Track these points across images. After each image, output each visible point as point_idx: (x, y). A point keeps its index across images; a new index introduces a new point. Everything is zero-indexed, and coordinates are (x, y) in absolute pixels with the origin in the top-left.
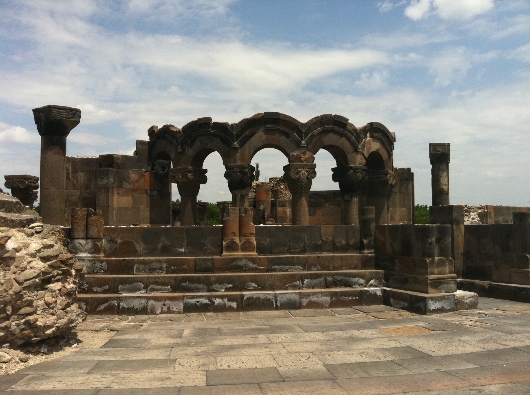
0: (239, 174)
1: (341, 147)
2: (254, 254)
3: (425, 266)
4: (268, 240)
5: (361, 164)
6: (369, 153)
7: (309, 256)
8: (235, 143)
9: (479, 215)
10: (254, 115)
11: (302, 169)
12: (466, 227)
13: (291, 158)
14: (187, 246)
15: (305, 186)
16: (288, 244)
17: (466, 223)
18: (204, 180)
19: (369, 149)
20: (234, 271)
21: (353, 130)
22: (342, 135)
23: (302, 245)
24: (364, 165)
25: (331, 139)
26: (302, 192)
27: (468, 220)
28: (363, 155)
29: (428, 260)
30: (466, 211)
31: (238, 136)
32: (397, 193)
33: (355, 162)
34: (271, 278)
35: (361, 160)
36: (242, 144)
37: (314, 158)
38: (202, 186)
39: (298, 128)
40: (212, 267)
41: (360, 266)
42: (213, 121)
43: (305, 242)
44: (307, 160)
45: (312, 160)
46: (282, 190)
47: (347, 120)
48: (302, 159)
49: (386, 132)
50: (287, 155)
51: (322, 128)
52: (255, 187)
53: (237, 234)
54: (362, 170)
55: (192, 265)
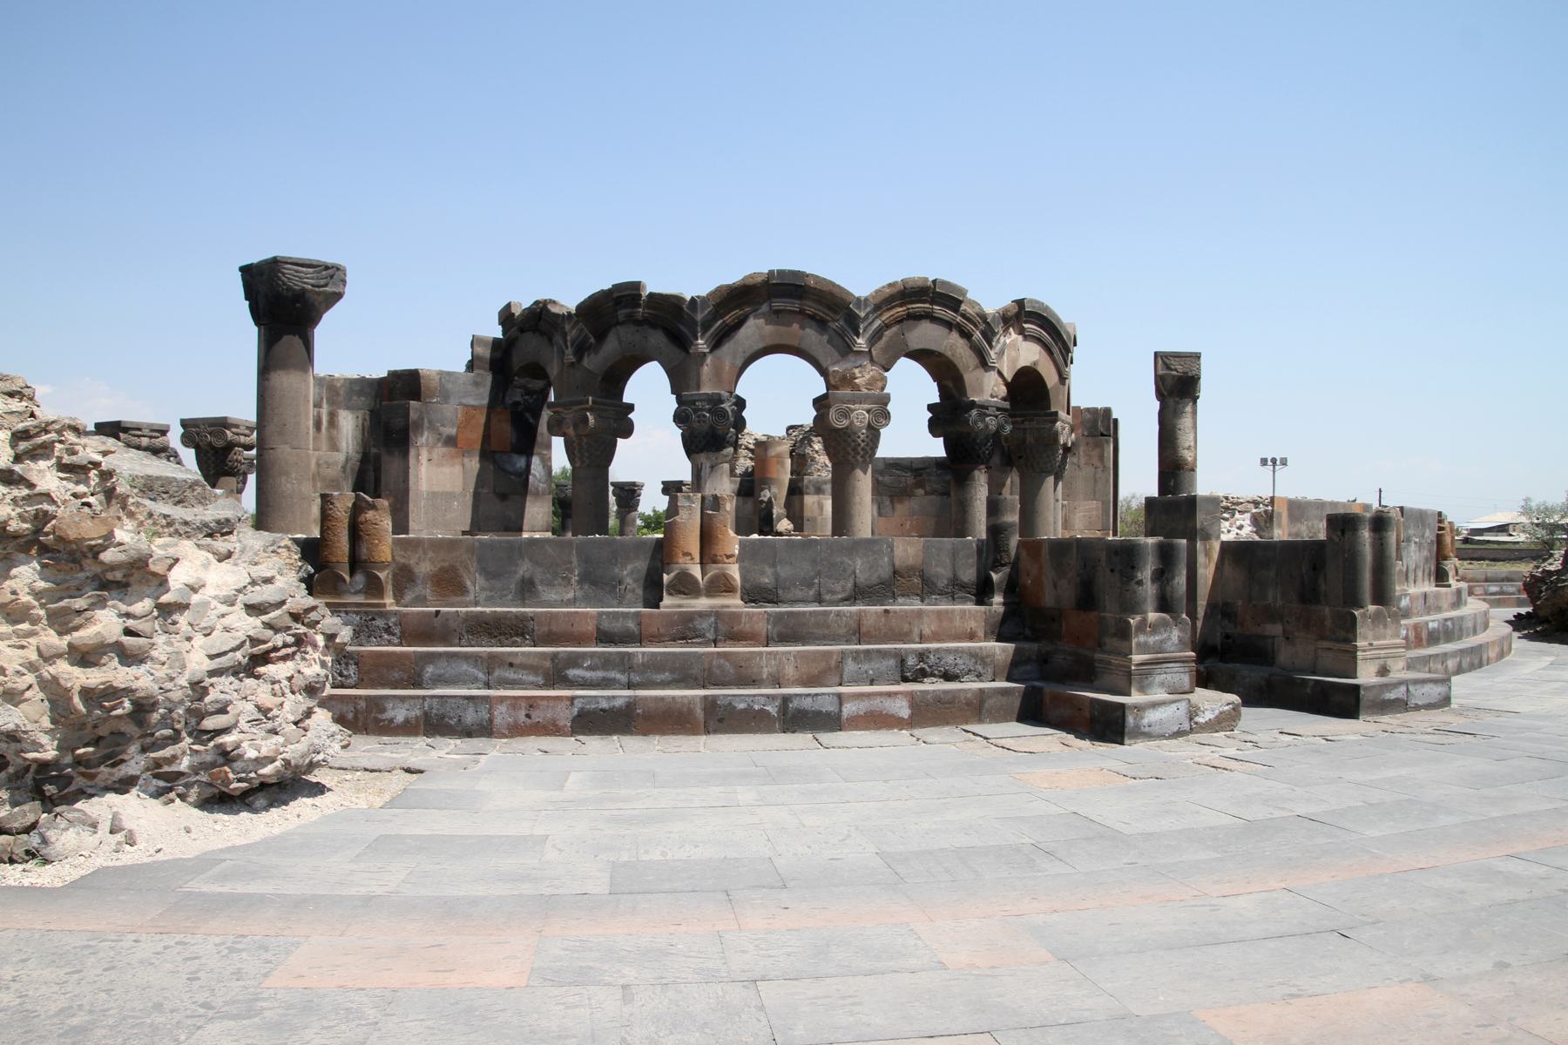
0: (708, 415)
1: (949, 354)
2: (734, 603)
3: (1124, 633)
4: (769, 571)
5: (997, 397)
6: (1016, 370)
7: (864, 611)
8: (700, 341)
9: (1255, 520)
10: (745, 277)
11: (857, 406)
12: (1226, 546)
13: (831, 378)
14: (579, 582)
15: (863, 444)
16: (816, 581)
17: (1224, 537)
18: (627, 430)
19: (1014, 361)
20: (687, 643)
21: (978, 315)
22: (949, 325)
23: (850, 585)
24: (1004, 399)
25: (926, 335)
26: (857, 460)
27: (1229, 531)
28: (1000, 374)
29: (1133, 619)
30: (1227, 509)
31: (706, 326)
32: (1079, 466)
33: (981, 391)
34: (775, 659)
35: (994, 386)
36: (717, 343)
37: (884, 379)
38: (620, 441)
39: (848, 308)
40: (637, 633)
41: (981, 634)
43: (855, 577)
44: (871, 384)
45: (880, 384)
46: (816, 455)
47: (963, 292)
48: (856, 381)
49: (1054, 322)
50: (823, 372)
51: (905, 308)
52: (752, 447)
53: (697, 559)
54: (998, 409)
55: (590, 627)
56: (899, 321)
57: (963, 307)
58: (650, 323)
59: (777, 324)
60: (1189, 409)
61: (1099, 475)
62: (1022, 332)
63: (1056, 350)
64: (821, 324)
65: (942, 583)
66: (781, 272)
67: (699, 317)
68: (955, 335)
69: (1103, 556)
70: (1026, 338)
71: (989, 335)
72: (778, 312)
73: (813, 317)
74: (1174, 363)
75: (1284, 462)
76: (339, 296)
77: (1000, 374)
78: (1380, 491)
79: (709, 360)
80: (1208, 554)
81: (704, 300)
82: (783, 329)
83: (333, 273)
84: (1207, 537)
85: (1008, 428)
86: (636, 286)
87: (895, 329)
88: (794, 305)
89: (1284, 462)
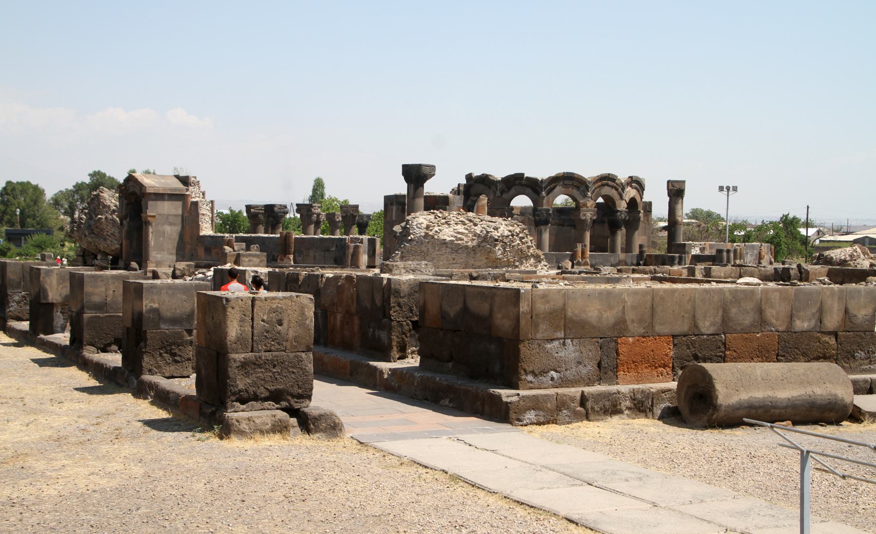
9: (700, 249)
12: (693, 256)
17: (692, 253)
22: (612, 187)
28: (626, 201)
31: (545, 188)
36: (548, 194)
42: (525, 176)
47: (617, 177)
56: (599, 187)
57: (616, 181)
58: (527, 186)
59: (565, 188)
60: (680, 201)
61: (647, 226)
62: (631, 186)
63: (640, 191)
64: (578, 188)
65: (629, 264)
66: (567, 173)
67: (544, 186)
68: (614, 190)
69: (667, 258)
70: (632, 188)
71: (623, 189)
72: (565, 184)
73: (575, 186)
74: (675, 184)
75: (735, 189)
76: (434, 175)
77: (626, 201)
78: (808, 207)
79: (546, 198)
80: (688, 257)
81: (546, 180)
82: (567, 189)
83: (433, 168)
84: (688, 253)
85: (627, 218)
86: (523, 174)
87: (598, 189)
88: (571, 182)
89: (735, 189)
